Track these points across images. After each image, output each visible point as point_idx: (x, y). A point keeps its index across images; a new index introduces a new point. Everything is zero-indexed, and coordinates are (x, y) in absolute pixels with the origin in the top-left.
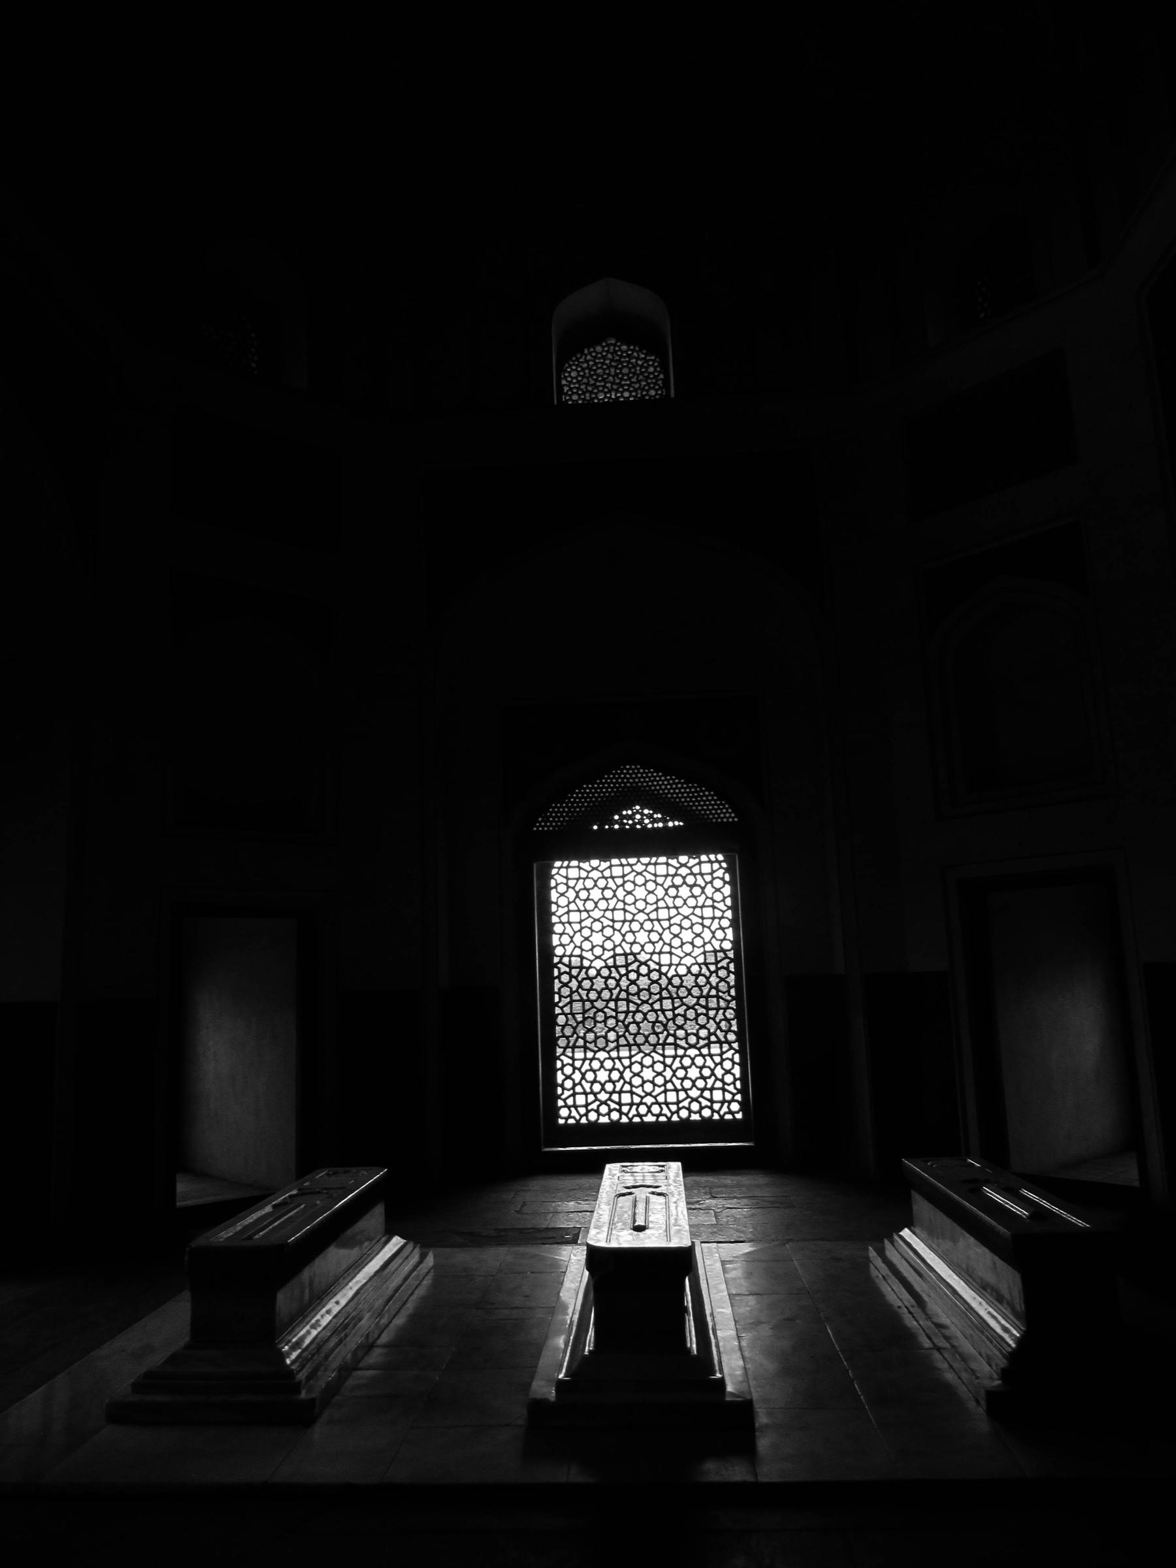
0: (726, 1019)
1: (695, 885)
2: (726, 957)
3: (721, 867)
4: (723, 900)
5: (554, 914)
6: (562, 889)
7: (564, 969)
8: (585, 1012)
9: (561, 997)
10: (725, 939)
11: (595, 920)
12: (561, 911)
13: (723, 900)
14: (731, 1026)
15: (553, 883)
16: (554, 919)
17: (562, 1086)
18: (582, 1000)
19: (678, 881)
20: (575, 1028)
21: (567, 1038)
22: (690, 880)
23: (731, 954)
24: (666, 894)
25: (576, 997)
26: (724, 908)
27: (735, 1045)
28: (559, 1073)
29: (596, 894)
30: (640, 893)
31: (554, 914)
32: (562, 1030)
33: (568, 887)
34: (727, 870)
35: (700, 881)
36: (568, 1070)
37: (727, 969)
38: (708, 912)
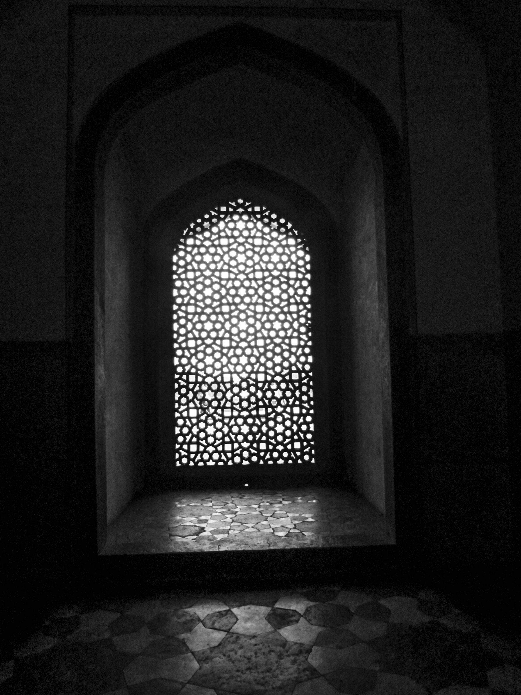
0: (305, 422)
1: (286, 320)
6: (182, 322)
7: (182, 383)
12: (181, 339)
14: (309, 428)
16: (176, 346)
32: (181, 431)
38: (295, 342)
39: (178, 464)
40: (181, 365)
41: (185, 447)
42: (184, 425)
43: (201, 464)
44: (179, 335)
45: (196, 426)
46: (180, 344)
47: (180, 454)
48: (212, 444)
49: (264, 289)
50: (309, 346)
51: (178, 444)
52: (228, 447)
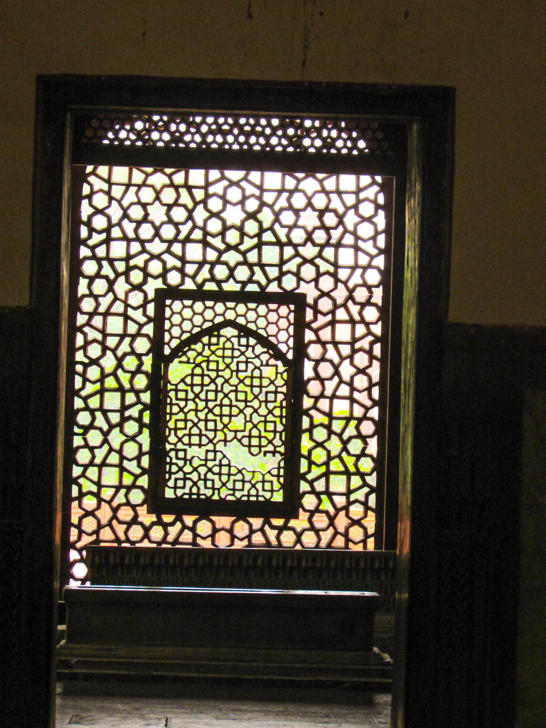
0: (360, 436)
2: (369, 333)
3: (374, 183)
4: (374, 238)
5: (84, 242)
7: (93, 334)
8: (124, 408)
9: (85, 380)
10: (368, 303)
11: (153, 257)
12: (96, 238)
13: (374, 238)
15: (86, 190)
17: (79, 527)
18: (121, 389)
19: (299, 201)
20: (106, 434)
21: (92, 449)
23: (377, 329)
24: (277, 220)
25: (110, 382)
26: (374, 252)
27: (372, 480)
28: (75, 504)
29: (157, 213)
30: (234, 215)
31: (84, 242)
33: (111, 199)
34: (384, 187)
35: (336, 203)
36: (90, 502)
37: (370, 353)
40: (91, 294)
44: (92, 230)
45: (118, 429)
47: (80, 486)
51: (78, 465)
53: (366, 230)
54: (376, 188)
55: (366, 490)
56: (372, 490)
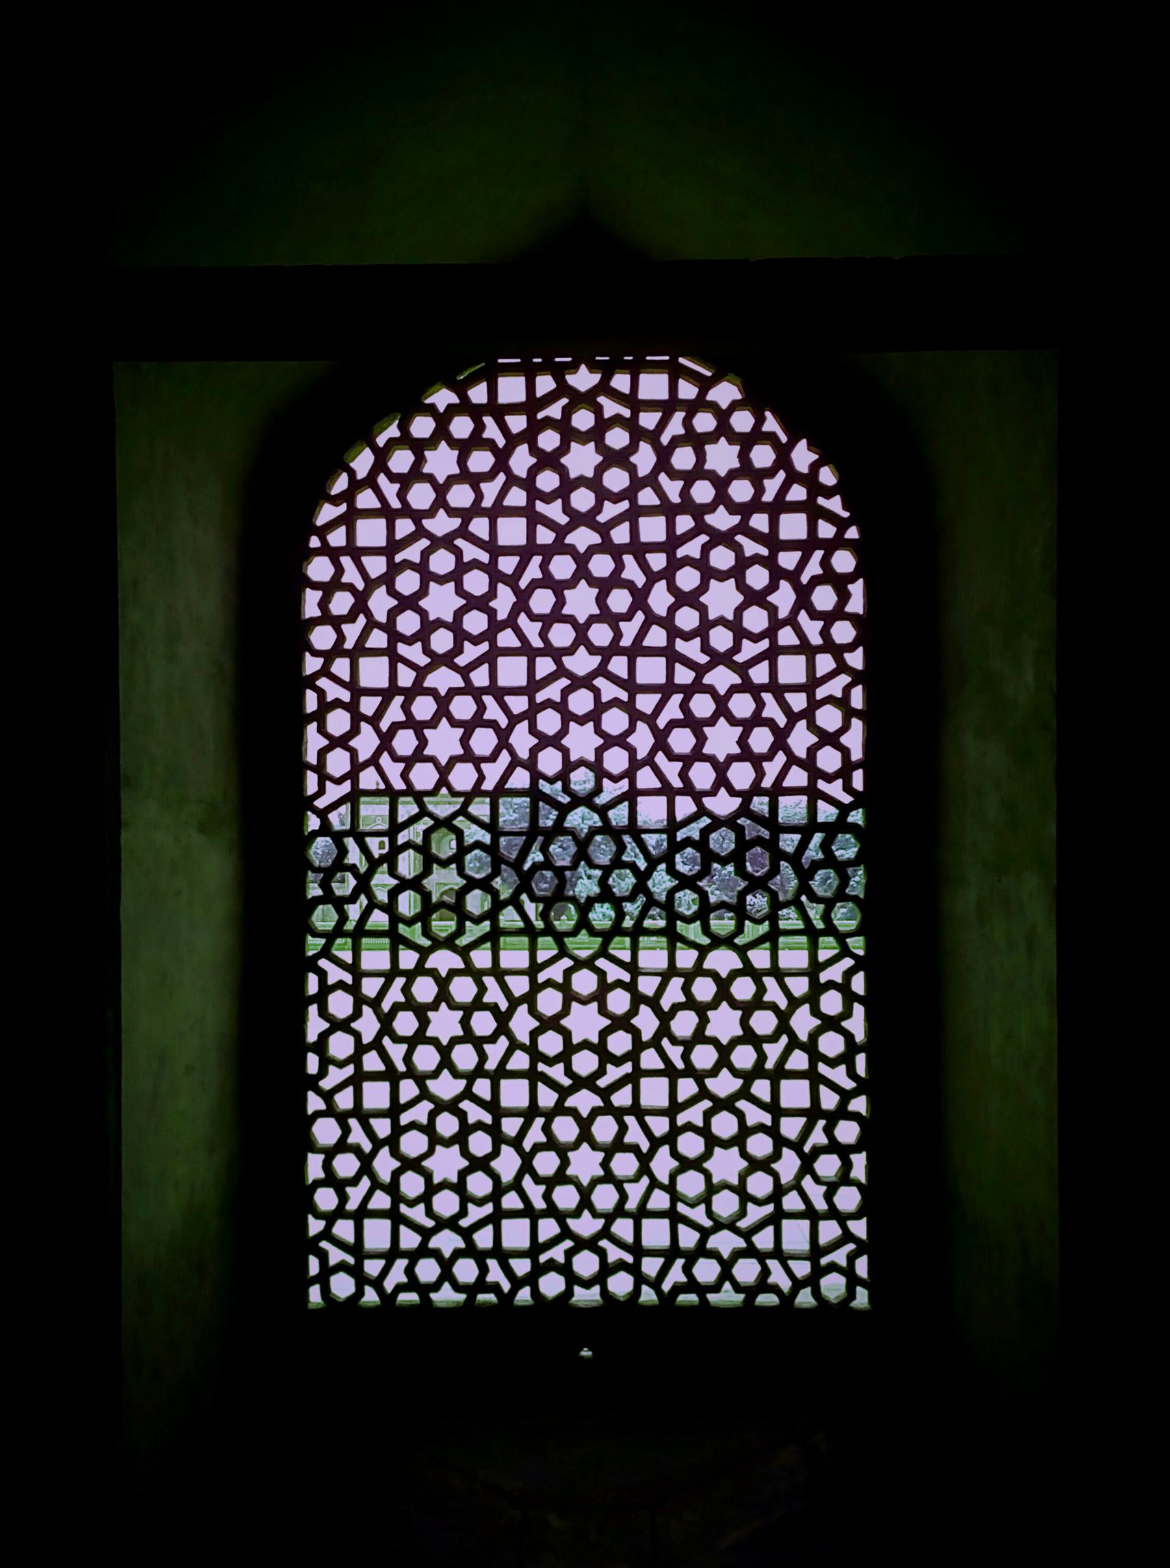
0: (834, 1146)
3: (842, 667)
12: (334, 792)
22: (742, 706)
39: (315, 1295)
40: (328, 897)
41: (344, 1229)
42: (342, 1146)
43: (409, 1298)
46: (323, 814)
48: (452, 1224)
49: (672, 588)
50: (853, 829)
52: (516, 1234)
53: (829, 760)
54: (844, 679)
55: (851, 1246)
56: (862, 1248)
